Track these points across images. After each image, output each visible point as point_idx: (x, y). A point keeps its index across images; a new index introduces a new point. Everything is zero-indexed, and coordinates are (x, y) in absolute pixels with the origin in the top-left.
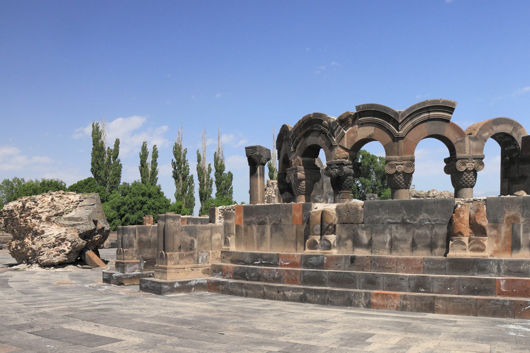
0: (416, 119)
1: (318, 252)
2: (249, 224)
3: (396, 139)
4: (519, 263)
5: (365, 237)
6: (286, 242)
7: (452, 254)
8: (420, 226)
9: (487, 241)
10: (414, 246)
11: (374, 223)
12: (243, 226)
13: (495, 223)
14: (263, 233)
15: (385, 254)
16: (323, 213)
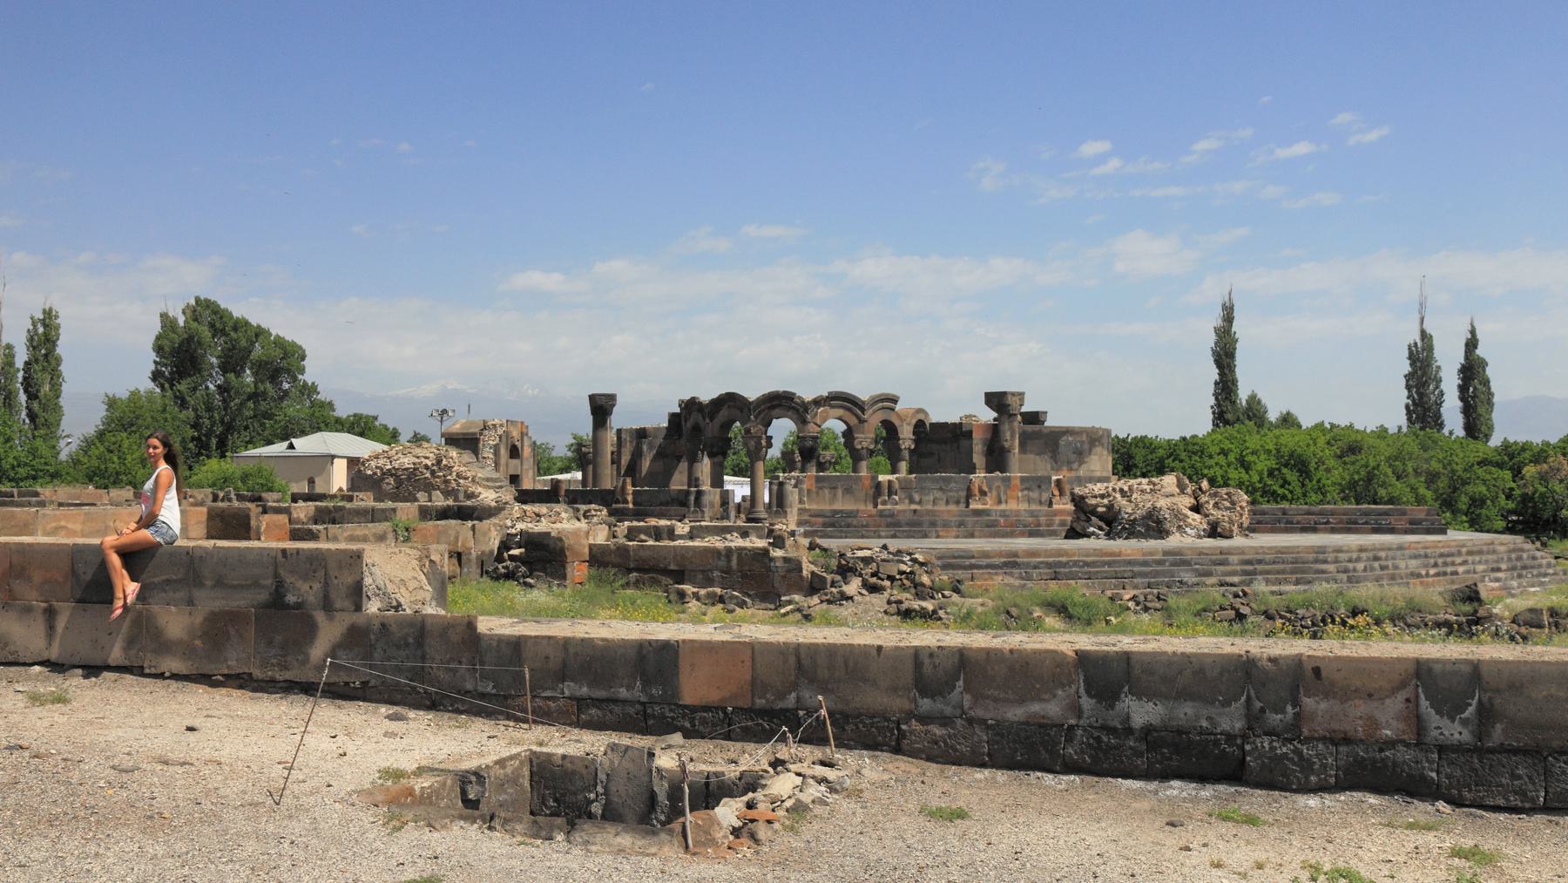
0: (875, 407)
1: (889, 507)
2: (821, 488)
3: (861, 421)
4: (1004, 511)
5: (917, 497)
6: (857, 500)
7: (971, 507)
8: (951, 491)
9: (988, 499)
10: (947, 503)
11: (923, 488)
12: (814, 490)
13: (990, 489)
14: (835, 495)
15: (930, 507)
16: (890, 482)
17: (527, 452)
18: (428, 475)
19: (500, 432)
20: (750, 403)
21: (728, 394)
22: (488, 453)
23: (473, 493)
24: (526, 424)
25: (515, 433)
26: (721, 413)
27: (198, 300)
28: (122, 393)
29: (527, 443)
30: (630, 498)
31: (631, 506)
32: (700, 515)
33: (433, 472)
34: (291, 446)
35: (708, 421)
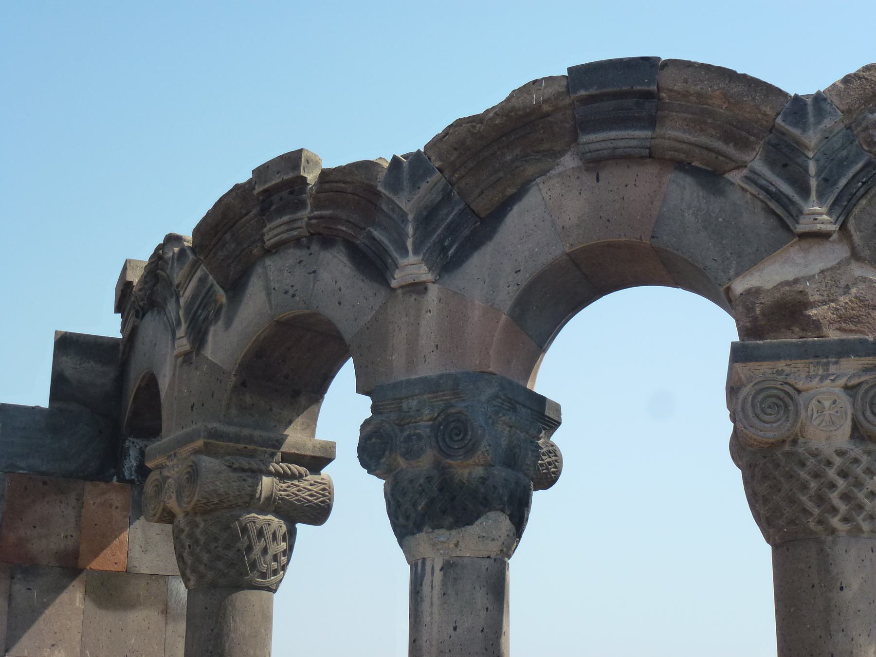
26: (514, 218)
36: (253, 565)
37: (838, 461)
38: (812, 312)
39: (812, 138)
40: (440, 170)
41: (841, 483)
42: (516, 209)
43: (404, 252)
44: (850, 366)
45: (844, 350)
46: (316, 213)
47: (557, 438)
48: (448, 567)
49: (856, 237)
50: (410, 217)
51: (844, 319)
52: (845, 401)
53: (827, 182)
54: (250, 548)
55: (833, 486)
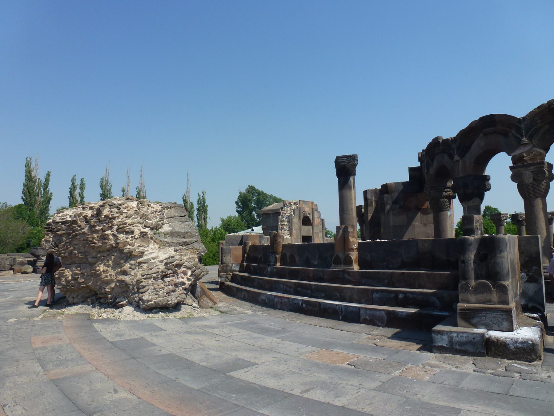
17: (317, 221)
18: (86, 230)
19: (294, 207)
20: (519, 120)
21: (482, 119)
22: (283, 221)
23: (130, 252)
24: (315, 203)
25: (307, 209)
27: (249, 186)
28: (225, 218)
29: (316, 216)
30: (354, 256)
31: (356, 268)
32: (495, 296)
33: (91, 227)
34: (253, 230)
35: (457, 157)
36: (443, 207)
37: (530, 185)
38: (525, 158)
39: (523, 126)
40: (459, 139)
41: (531, 189)
42: (473, 145)
43: (455, 155)
44: (532, 168)
45: (531, 165)
46: (443, 147)
47: (490, 182)
48: (468, 208)
49: (534, 142)
50: (455, 148)
51: (531, 159)
52: (531, 175)
53: (527, 133)
54: (441, 205)
55: (530, 189)
